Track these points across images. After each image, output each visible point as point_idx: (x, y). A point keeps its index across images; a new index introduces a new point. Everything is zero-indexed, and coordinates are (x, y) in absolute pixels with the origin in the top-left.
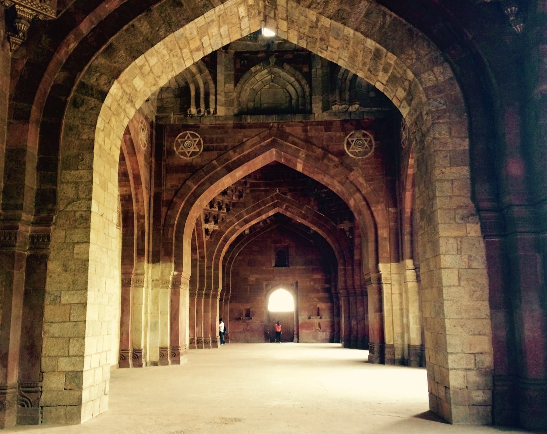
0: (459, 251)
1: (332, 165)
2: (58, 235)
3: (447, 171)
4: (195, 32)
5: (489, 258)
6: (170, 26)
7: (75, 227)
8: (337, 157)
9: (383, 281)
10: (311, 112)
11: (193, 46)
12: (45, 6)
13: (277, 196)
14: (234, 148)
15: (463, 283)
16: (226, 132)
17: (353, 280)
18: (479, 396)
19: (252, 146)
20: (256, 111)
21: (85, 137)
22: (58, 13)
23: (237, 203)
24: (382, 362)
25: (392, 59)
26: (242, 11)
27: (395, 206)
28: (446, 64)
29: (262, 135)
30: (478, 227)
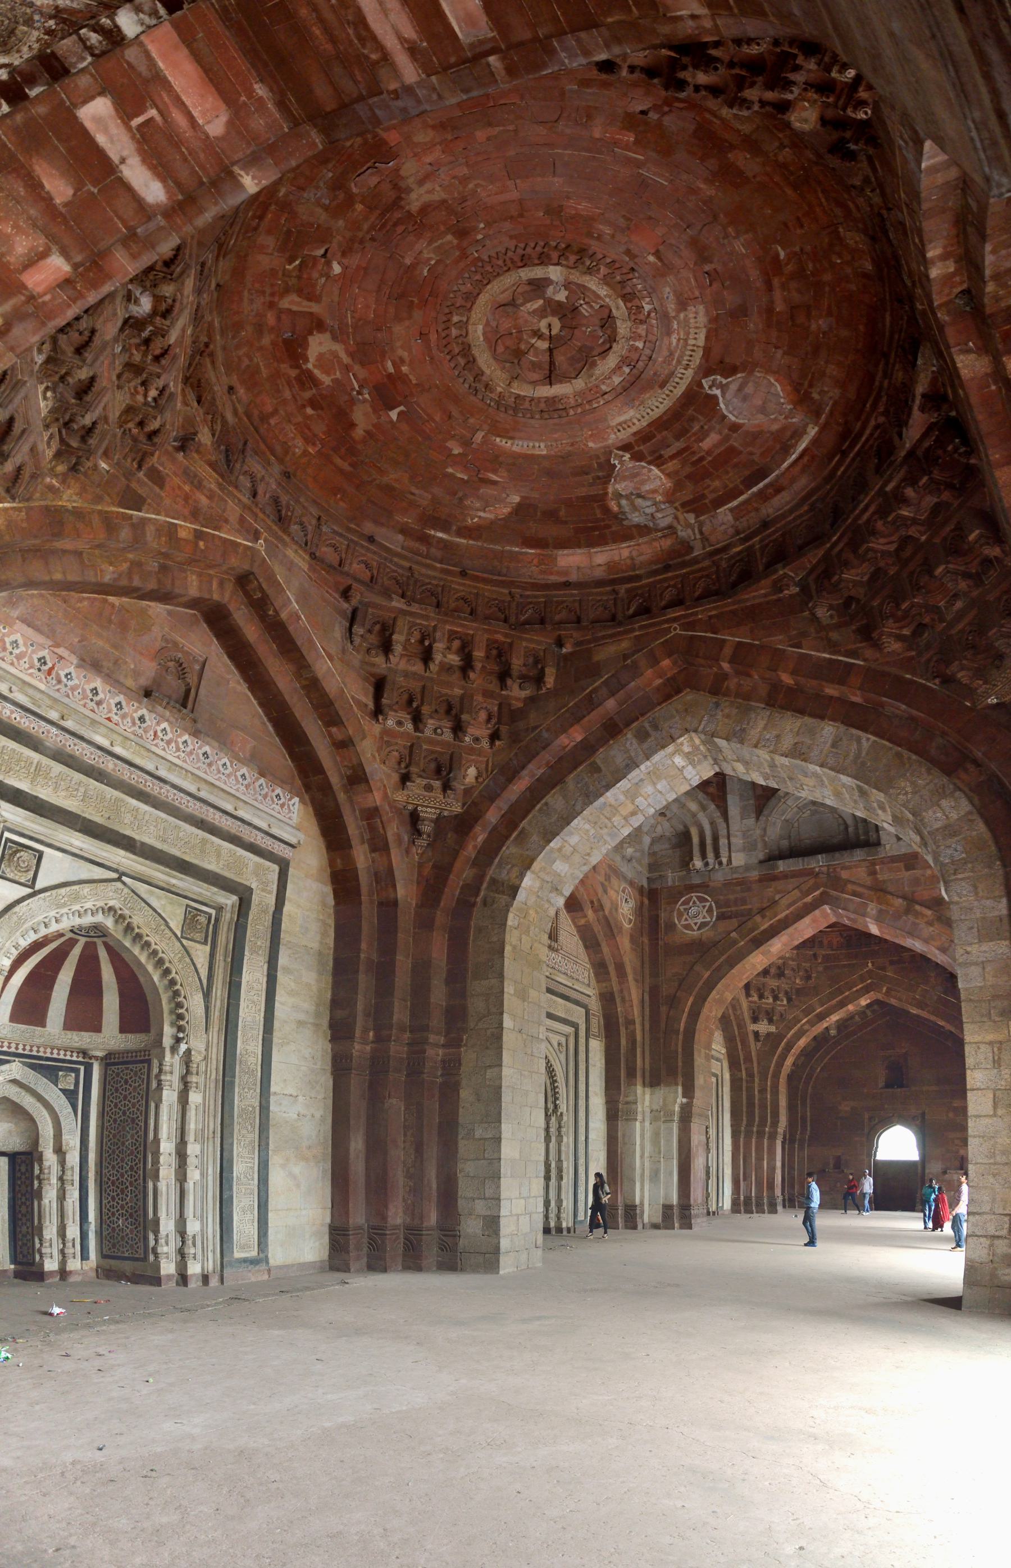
4: (622, 797)
6: (587, 796)
11: (624, 811)
12: (449, 801)
22: (464, 805)
26: (679, 761)
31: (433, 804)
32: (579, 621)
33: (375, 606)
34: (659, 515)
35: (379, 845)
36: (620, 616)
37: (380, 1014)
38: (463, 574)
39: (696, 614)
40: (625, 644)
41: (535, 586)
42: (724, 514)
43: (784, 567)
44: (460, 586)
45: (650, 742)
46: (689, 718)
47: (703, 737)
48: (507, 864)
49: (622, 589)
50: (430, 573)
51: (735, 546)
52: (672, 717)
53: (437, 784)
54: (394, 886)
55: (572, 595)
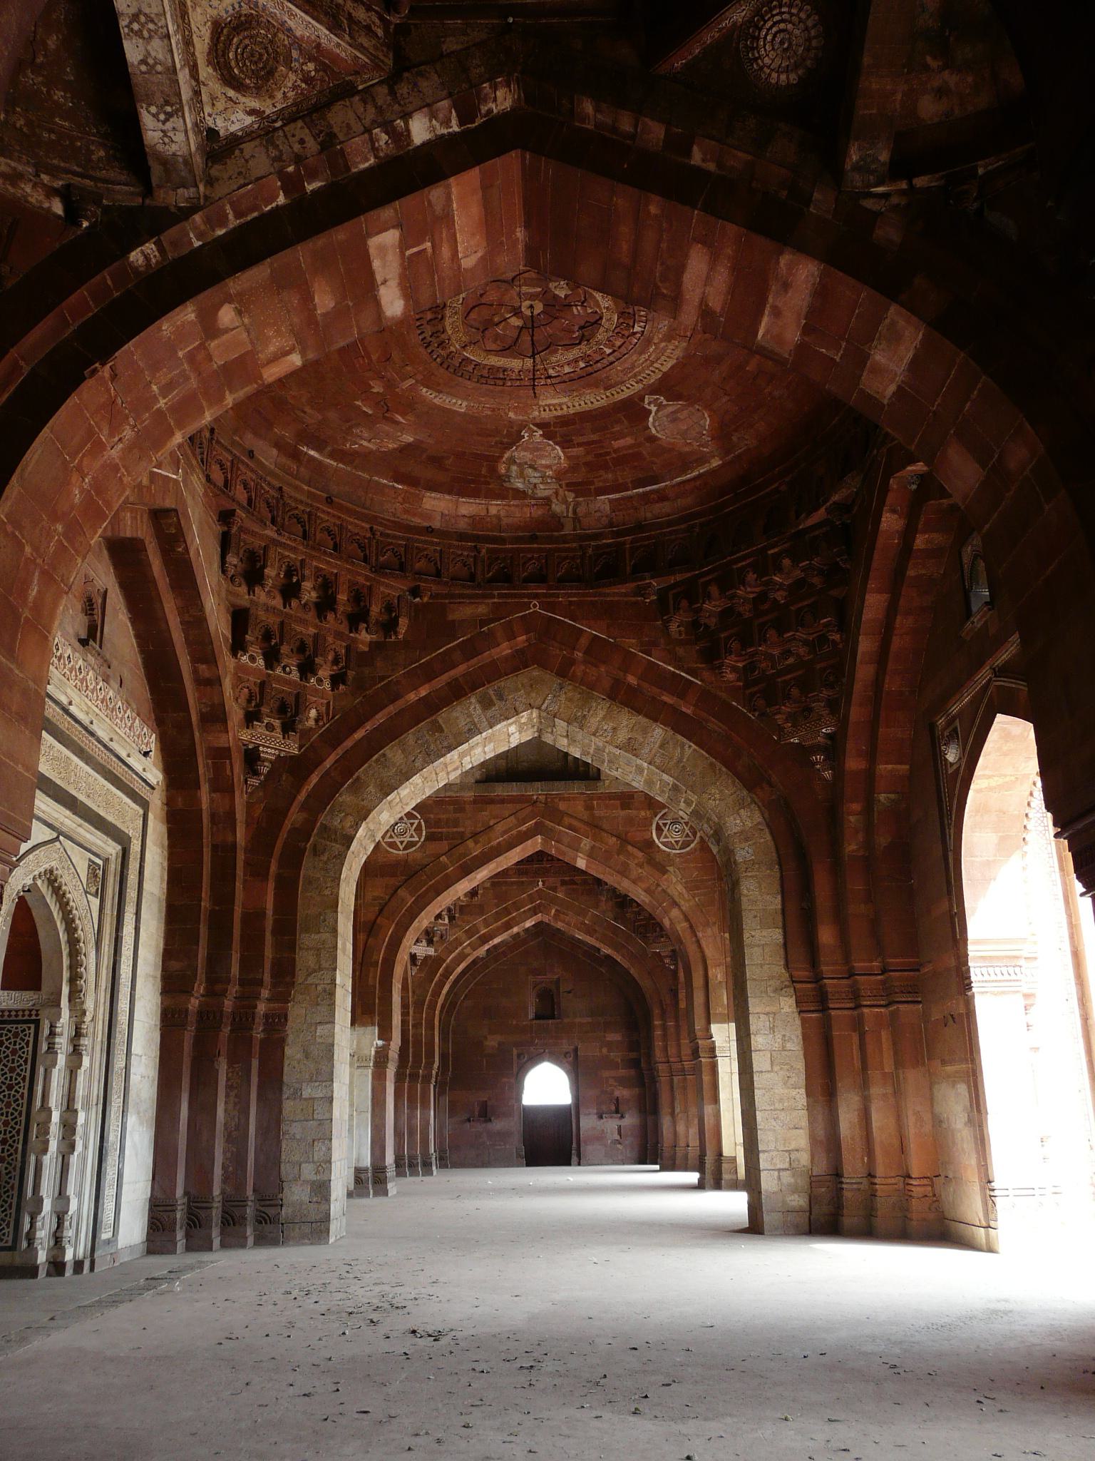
0: (772, 1029)
2: (297, 1012)
3: (757, 934)
5: (805, 1038)
14: (475, 835)
15: (776, 1068)
16: (462, 810)
17: (679, 1045)
19: (505, 832)
21: (327, 892)
22: (300, 748)
23: (467, 906)
24: (718, 1186)
25: (694, 798)
26: (512, 729)
29: (521, 815)
30: (792, 1001)
31: (273, 744)
32: (438, 574)
33: (254, 534)
35: (223, 786)
38: (329, 500)
40: (482, 609)
42: (603, 502)
44: (327, 517)
45: (492, 711)
47: (544, 714)
49: (485, 548)
50: (298, 496)
52: (517, 690)
53: (277, 723)
55: (433, 543)
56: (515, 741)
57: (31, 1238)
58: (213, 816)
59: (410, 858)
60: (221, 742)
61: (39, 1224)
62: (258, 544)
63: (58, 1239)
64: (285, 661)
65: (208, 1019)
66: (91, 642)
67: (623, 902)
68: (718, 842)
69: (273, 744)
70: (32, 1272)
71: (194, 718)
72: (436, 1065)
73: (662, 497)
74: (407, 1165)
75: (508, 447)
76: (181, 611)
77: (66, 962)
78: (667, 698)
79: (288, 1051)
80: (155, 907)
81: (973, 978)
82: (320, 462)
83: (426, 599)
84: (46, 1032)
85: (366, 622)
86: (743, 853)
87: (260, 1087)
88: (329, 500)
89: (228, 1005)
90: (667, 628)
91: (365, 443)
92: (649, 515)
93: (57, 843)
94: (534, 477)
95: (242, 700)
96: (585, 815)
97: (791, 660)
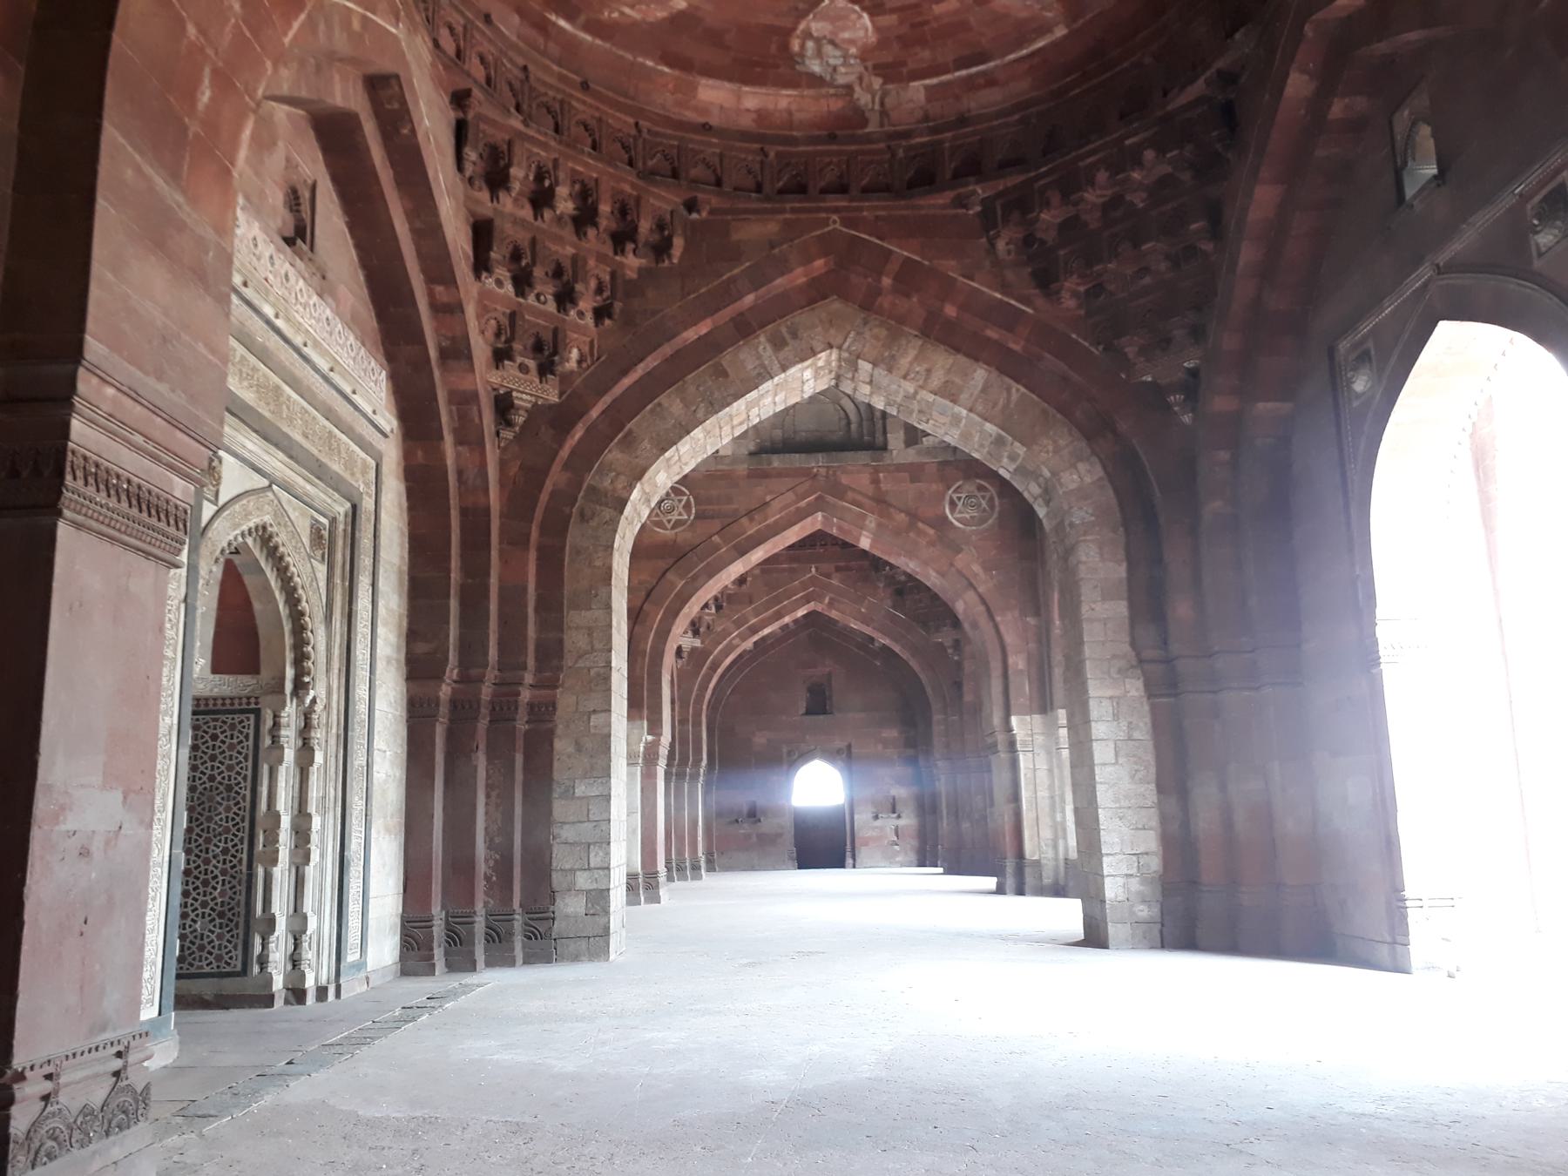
0: (1116, 717)
1: (923, 542)
2: (566, 701)
3: (1098, 607)
7: (591, 690)
8: (932, 527)
9: (1019, 747)
10: (884, 448)
11: (735, 422)
13: (813, 581)
15: (1121, 760)
18: (1143, 911)
20: (788, 446)
21: (598, 563)
25: (1021, 450)
26: (808, 374)
27: (1037, 613)
28: (1094, 459)
29: (801, 489)
30: (1140, 684)
31: (530, 391)
32: (719, 183)
33: (492, 123)
34: (843, 70)
35: (469, 437)
36: (767, 188)
37: (471, 650)
38: (585, 86)
39: (861, 209)
40: (772, 227)
41: (669, 121)
43: (977, 183)
44: (583, 107)
45: (787, 352)
46: (832, 331)
47: (845, 355)
48: (610, 470)
51: (921, 136)
53: (532, 364)
54: (486, 490)
56: (809, 390)
57: (263, 961)
58: (460, 473)
59: (679, 539)
60: (465, 385)
61: (272, 946)
62: (500, 137)
63: (295, 961)
64: (538, 288)
65: (462, 709)
66: (299, 242)
67: (906, 589)
68: (1047, 503)
69: (530, 391)
70: (268, 1001)
71: (433, 353)
72: (704, 762)
73: (990, 81)
74: (681, 868)
75: (803, 15)
76: (410, 215)
77: (288, 641)
78: (992, 333)
79: (558, 745)
80: (394, 578)
81: (1381, 653)
82: (574, 37)
83: (704, 214)
84: (269, 723)
85: (634, 241)
86: (1080, 515)
87: (526, 785)
88: (585, 86)
89: (486, 691)
90: (993, 245)
91: (627, 10)
92: (973, 105)
93: (270, 494)
94: (833, 56)
95: (490, 334)
96: (870, 490)
97: (1147, 280)
